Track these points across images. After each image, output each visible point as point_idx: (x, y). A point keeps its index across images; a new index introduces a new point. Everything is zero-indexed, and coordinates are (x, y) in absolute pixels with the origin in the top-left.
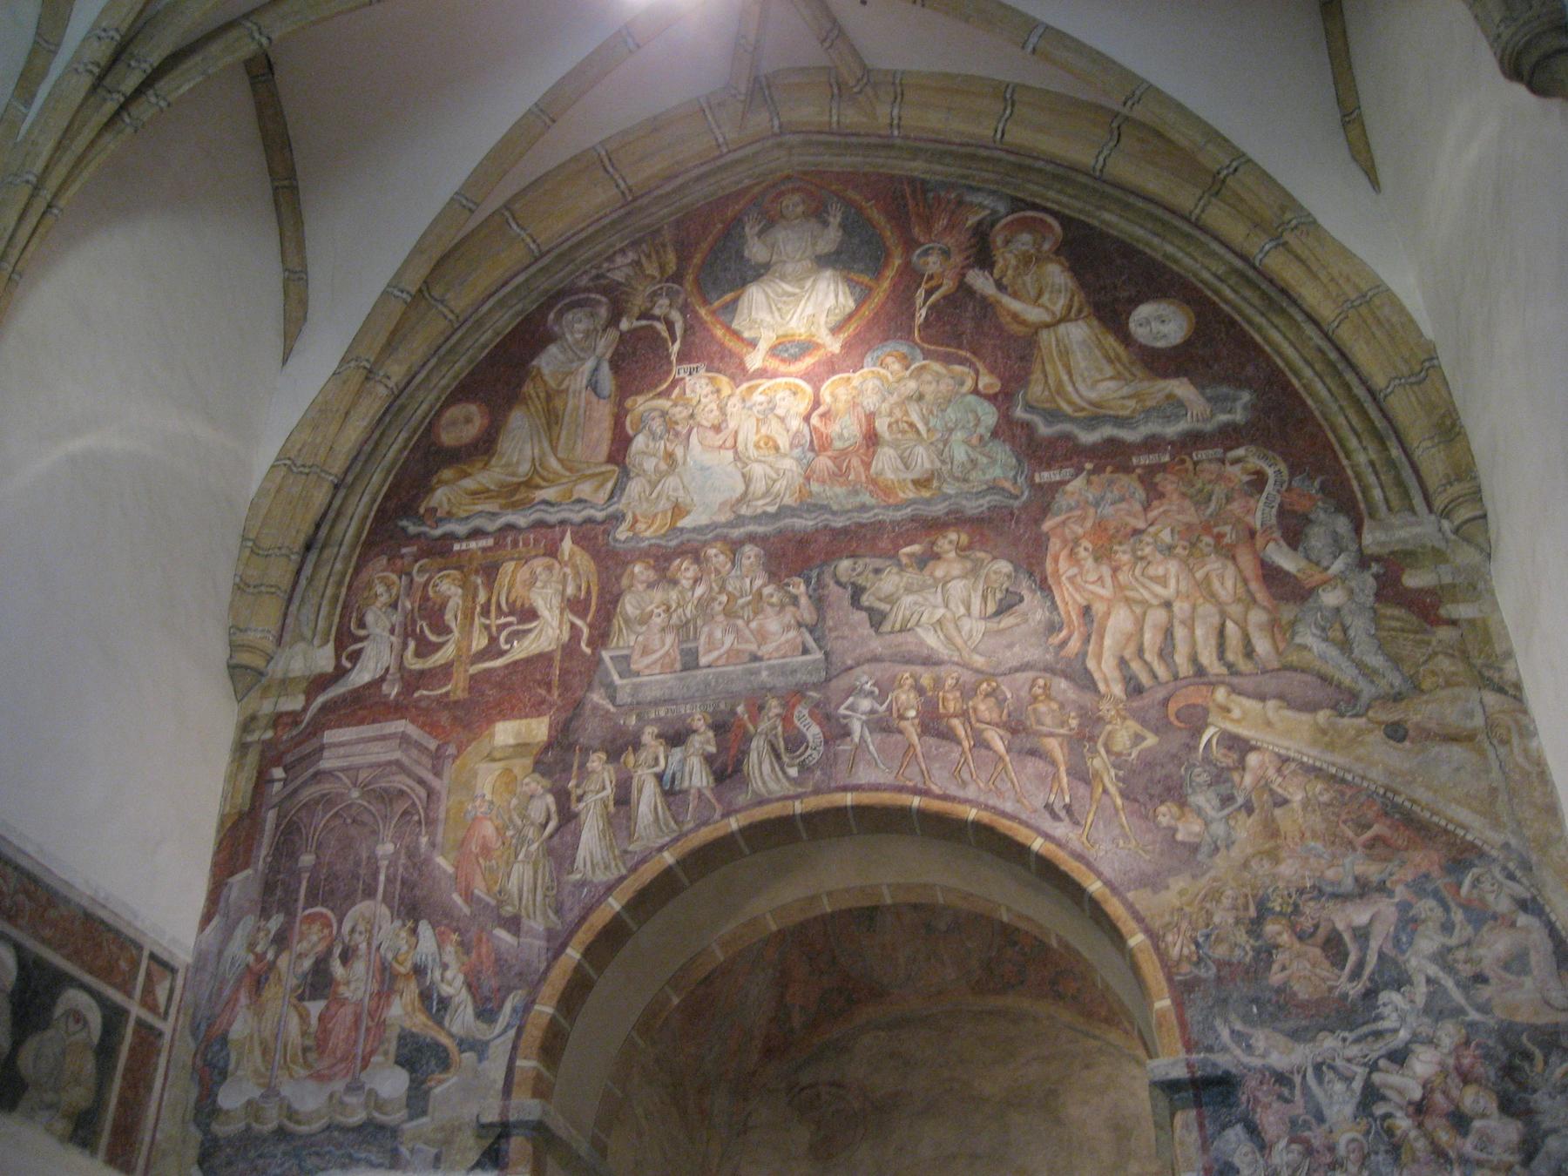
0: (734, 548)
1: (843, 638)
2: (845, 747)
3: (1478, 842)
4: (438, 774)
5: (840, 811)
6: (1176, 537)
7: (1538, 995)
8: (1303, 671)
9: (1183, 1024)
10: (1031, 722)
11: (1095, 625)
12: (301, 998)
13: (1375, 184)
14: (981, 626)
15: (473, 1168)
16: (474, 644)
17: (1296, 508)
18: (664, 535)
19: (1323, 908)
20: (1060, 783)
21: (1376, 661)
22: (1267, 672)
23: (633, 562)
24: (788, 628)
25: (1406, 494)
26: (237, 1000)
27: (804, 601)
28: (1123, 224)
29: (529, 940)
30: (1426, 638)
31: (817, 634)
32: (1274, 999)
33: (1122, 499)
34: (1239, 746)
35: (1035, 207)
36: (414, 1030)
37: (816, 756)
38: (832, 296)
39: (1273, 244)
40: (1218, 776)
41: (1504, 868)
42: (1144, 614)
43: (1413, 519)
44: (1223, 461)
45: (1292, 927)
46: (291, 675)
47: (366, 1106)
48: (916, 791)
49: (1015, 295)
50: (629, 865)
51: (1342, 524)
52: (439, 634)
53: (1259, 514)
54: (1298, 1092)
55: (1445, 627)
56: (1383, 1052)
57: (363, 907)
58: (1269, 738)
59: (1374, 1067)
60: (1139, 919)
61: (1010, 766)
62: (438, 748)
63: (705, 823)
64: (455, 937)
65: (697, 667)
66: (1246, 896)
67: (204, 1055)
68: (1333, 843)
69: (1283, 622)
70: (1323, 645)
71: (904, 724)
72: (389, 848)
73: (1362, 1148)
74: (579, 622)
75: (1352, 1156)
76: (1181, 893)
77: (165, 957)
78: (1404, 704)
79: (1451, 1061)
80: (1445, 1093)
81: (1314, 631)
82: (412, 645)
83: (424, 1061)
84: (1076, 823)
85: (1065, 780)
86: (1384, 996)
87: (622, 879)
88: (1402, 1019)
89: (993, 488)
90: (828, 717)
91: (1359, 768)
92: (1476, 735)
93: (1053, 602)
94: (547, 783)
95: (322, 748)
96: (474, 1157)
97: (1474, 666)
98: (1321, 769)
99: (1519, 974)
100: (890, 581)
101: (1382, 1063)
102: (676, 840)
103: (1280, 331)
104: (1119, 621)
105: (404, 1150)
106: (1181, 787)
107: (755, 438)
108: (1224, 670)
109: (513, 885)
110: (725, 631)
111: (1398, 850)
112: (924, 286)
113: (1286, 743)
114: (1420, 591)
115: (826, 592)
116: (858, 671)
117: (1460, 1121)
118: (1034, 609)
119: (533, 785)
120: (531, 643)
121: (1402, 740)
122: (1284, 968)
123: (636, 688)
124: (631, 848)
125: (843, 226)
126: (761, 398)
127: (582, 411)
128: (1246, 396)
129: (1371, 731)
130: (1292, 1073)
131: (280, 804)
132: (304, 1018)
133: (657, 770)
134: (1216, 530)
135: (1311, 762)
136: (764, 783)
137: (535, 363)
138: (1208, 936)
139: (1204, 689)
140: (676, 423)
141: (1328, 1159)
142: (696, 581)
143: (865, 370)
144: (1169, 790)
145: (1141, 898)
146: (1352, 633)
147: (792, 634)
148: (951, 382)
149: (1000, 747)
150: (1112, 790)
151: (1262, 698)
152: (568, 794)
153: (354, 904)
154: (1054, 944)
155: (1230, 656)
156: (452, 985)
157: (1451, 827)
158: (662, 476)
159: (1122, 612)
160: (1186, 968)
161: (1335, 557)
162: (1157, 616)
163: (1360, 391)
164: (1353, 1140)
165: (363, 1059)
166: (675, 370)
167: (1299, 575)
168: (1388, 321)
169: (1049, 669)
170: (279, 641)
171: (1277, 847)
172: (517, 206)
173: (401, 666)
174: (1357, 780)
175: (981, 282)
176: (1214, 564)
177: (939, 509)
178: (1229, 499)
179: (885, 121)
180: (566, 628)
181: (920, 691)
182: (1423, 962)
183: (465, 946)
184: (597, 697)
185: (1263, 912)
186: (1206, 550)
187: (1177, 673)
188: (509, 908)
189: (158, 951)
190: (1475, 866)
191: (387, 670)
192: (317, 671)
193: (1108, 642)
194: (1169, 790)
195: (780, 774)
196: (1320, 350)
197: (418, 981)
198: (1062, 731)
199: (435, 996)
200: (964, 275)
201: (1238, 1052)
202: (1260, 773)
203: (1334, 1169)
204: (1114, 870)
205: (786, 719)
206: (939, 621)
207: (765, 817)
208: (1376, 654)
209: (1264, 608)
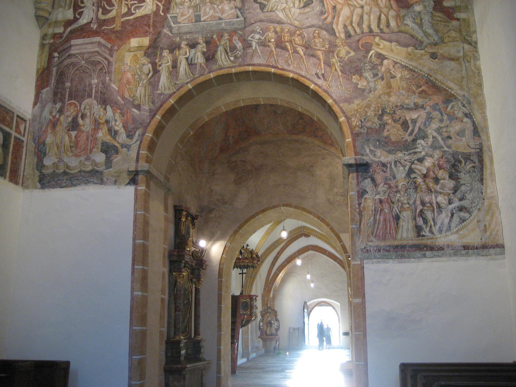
1: (250, 13)
2: (250, 51)
3: (455, 94)
4: (111, 56)
7: (466, 144)
8: (406, 33)
10: (313, 45)
11: (337, 12)
12: (68, 130)
14: (298, 11)
15: (127, 184)
16: (123, 10)
19: (403, 112)
20: (321, 66)
21: (430, 31)
22: (394, 33)
24: (232, 8)
26: (47, 131)
29: (143, 112)
30: (448, 24)
31: (242, 11)
32: (384, 140)
34: (381, 57)
36: (106, 141)
37: (240, 53)
40: (374, 67)
41: (462, 103)
42: (354, 10)
45: (392, 118)
46: (58, 20)
47: (92, 165)
48: (273, 67)
50: (176, 88)
52: (110, 7)
54: (388, 169)
55: (455, 21)
56: (415, 159)
57: (87, 101)
58: (391, 55)
59: (413, 163)
60: (343, 112)
61: (305, 60)
62: (111, 47)
63: (202, 75)
64: (119, 111)
65: (200, 21)
67: (38, 149)
68: (408, 91)
69: (401, 16)
70: (413, 25)
71: (270, 44)
72: (96, 81)
73: (406, 187)
74: (159, 4)
75: (403, 189)
76: (358, 105)
77: (22, 116)
78: (437, 46)
79: (437, 162)
80: (433, 172)
81: (411, 19)
82: (101, 10)
83: (110, 151)
84: (325, 80)
85: (323, 65)
86: (419, 141)
87: (174, 93)
88: (424, 149)
90: (245, 40)
92: (459, 59)
93: (323, 4)
94: (149, 60)
95: (71, 46)
96: (127, 181)
97: (463, 35)
98: (407, 67)
99: (461, 137)
101: (415, 162)
102: (192, 81)
104: (345, 12)
105: (105, 179)
106: (361, 70)
108: (379, 31)
109: (138, 94)
110: (210, 9)
111: (429, 95)
116: (254, 25)
117: (437, 180)
119: (144, 60)
120: (143, 11)
121: (436, 58)
122: (388, 131)
123: (179, 28)
124: (177, 83)
129: (425, 55)
130: (387, 163)
131: (57, 65)
132: (70, 137)
133: (186, 56)
135: (404, 64)
136: (222, 62)
138: (365, 119)
139: (372, 37)
141: (395, 190)
144: (357, 70)
145: (345, 106)
146: (423, 21)
147: (233, 11)
149: (302, 53)
150: (338, 69)
151: (391, 41)
152: (156, 64)
153: (85, 100)
154: (316, 119)
155: (382, 27)
156: (119, 126)
157: (447, 89)
159: (346, 9)
160: (357, 129)
162: (358, 11)
164: (404, 185)
165: (90, 150)
169: (320, 27)
170: (53, 7)
171: (390, 92)
173: (97, 18)
180: (155, 6)
181: (276, 32)
182: (432, 131)
183: (122, 114)
184: (166, 31)
185: (384, 112)
187: (363, 31)
188: (137, 102)
189: (19, 114)
190: (453, 102)
191: (92, 19)
192: (68, 18)
193: (341, 19)
194: (357, 70)
195: (228, 59)
197: (107, 126)
198: (323, 49)
199: (113, 130)
201: (371, 156)
202: (387, 67)
203: (397, 193)
204: (337, 96)
205: (230, 40)
206: (284, 9)
207: (222, 74)
209: (395, 10)
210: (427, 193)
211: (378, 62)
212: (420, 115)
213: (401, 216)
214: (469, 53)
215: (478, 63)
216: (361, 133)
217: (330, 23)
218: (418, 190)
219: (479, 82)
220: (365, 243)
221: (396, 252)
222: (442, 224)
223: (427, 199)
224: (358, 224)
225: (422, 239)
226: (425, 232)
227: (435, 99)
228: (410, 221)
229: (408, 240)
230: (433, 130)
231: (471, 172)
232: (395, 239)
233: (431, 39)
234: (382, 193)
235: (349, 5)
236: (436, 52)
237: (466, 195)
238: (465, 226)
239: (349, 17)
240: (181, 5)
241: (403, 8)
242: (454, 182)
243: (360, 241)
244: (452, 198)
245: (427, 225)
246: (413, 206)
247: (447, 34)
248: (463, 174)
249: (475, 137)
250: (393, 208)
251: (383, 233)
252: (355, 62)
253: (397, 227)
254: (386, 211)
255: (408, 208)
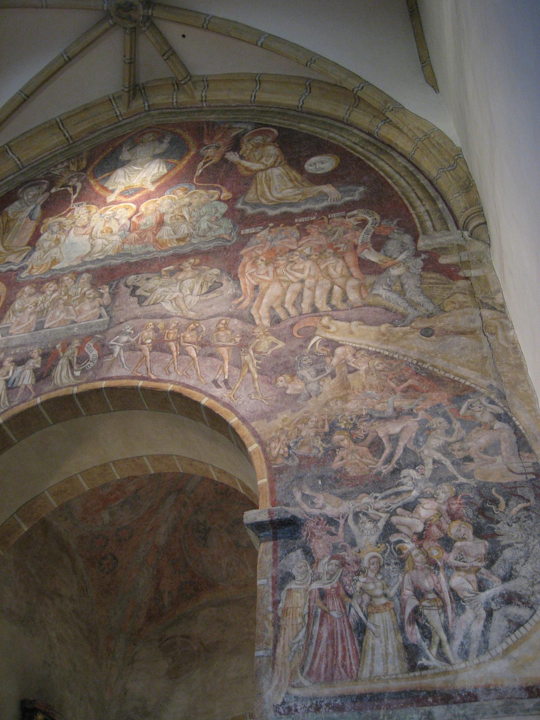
0: (77, 275)
1: (122, 310)
2: (108, 359)
3: (474, 386)
5: (98, 391)
6: (313, 251)
7: (505, 467)
8: (375, 306)
9: (272, 491)
10: (214, 341)
11: (260, 293)
13: (436, 88)
14: (197, 298)
17: (382, 233)
18: (44, 273)
19: (372, 425)
20: (224, 369)
21: (420, 299)
22: (354, 308)
23: (25, 286)
25: (445, 223)
27: (106, 295)
28: (310, 128)
31: (109, 309)
33: (286, 237)
35: (267, 126)
37: (92, 364)
38: (157, 169)
39: (383, 123)
40: (318, 360)
41: (488, 398)
42: (288, 287)
43: (448, 233)
44: (344, 217)
45: (351, 437)
48: (142, 378)
49: (248, 160)
51: (407, 238)
53: (361, 238)
54: (341, 529)
55: (461, 281)
56: (400, 504)
58: (350, 340)
59: (393, 513)
61: (197, 363)
65: (43, 328)
66: (324, 420)
68: (382, 391)
69: (367, 284)
70: (389, 294)
71: (144, 346)
73: (379, 563)
75: (372, 567)
79: (444, 508)
80: (439, 527)
81: (384, 287)
84: (229, 388)
86: (404, 472)
88: (415, 485)
89: (218, 238)
90: (103, 346)
91: (402, 352)
92: (475, 331)
93: (239, 285)
97: (478, 298)
98: (379, 353)
99: (493, 456)
100: (154, 282)
101: (399, 511)
103: (385, 161)
106: (294, 366)
107: (102, 229)
108: (329, 309)
111: (423, 392)
112: (203, 161)
113: (360, 342)
114: (448, 265)
115: (119, 290)
118: (228, 288)
121: (432, 335)
122: (342, 459)
125: (170, 143)
126: (111, 212)
127: (21, 226)
128: (362, 189)
130: (338, 518)
133: (7, 377)
134: (335, 247)
135: (374, 349)
136: (61, 380)
137: (6, 209)
140: (65, 226)
141: (356, 568)
142: (54, 291)
143: (165, 196)
144: (287, 368)
145: (260, 426)
146: (406, 287)
148: (207, 197)
149: (194, 354)
150: (253, 370)
151: (349, 321)
155: (334, 302)
157: (457, 379)
158: (50, 247)
160: (280, 461)
161: (401, 253)
162: (297, 287)
163: (424, 182)
164: (375, 557)
166: (72, 205)
167: (379, 263)
168: (438, 143)
171: (348, 394)
172: (12, 144)
174: (401, 357)
175: (232, 157)
176: (332, 261)
177: (188, 249)
178: (345, 233)
179: (198, 98)
181: (156, 330)
185: (333, 428)
186: (328, 255)
187: (302, 312)
190: (470, 398)
193: (265, 301)
195: (70, 375)
196: (406, 167)
200: (225, 155)
201: (305, 506)
203: (359, 575)
206: (175, 298)
208: (420, 295)
210: (426, 571)
211: (325, 353)
212: (407, 426)
213: (369, 625)
214: (492, 321)
215: (511, 333)
216: (287, 467)
217: (246, 308)
218: (407, 566)
219: (518, 361)
220: (285, 690)
221: (360, 710)
222: (467, 636)
223: (427, 584)
224: (271, 647)
225: (422, 677)
226: (428, 659)
227: (434, 397)
228: (391, 635)
229: (387, 681)
230: (434, 449)
231: (523, 519)
232: (356, 679)
233: (422, 310)
234: (325, 578)
235: (280, 280)
236: (431, 326)
237: (518, 567)
238: (524, 638)
239: (279, 296)
240: (20, 312)
241: (371, 275)
242: (487, 543)
243: (273, 686)
244: (485, 577)
245: (430, 641)
246: (397, 600)
247: (448, 300)
248: (506, 526)
249: (521, 453)
250: (351, 606)
251: (327, 665)
252: (285, 357)
253: (361, 651)
254: (335, 614)
255: (385, 605)
